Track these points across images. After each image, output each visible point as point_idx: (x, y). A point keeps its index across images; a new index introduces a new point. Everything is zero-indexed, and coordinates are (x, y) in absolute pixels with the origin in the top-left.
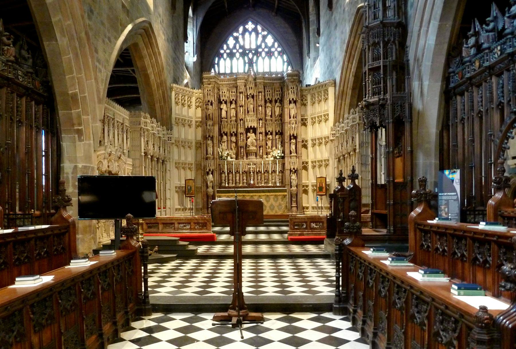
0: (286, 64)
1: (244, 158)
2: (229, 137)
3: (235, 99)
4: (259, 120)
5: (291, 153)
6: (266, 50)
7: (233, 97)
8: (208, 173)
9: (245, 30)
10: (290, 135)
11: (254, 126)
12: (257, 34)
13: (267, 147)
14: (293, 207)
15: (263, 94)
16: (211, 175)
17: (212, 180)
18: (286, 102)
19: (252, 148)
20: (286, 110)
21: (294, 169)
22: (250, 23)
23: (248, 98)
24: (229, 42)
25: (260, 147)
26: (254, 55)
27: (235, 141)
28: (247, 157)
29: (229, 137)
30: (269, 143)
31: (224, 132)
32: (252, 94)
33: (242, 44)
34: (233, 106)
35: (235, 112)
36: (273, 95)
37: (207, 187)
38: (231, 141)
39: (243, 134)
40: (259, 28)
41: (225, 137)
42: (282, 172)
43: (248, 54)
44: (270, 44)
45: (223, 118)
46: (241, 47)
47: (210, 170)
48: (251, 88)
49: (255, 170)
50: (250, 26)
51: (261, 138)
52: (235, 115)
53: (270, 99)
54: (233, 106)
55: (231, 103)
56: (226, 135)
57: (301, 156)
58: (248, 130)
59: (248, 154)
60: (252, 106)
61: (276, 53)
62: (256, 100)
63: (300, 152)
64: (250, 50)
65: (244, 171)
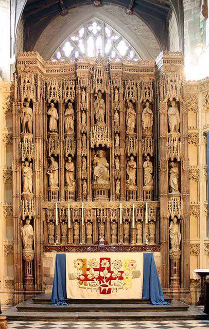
1: (88, 198)
2: (62, 163)
3: (72, 99)
4: (115, 134)
5: (170, 192)
7: (69, 95)
8: (24, 223)
9: (88, 33)
10: (170, 159)
11: (105, 145)
12: (105, 38)
13: (129, 181)
14: (173, 280)
15: (121, 91)
16: (30, 226)
17: (32, 234)
18: (162, 105)
20: (162, 117)
21: (176, 216)
22: (95, 24)
23: (96, 98)
24: (64, 49)
25: (116, 180)
27: (73, 170)
28: (93, 196)
29: (62, 163)
30: (132, 176)
31: (53, 155)
32: (103, 91)
33: (82, 50)
34: (70, 111)
35: (72, 122)
36: (139, 94)
37: (23, 247)
38: (65, 169)
39: (86, 158)
40: (108, 31)
41: (55, 164)
42: (157, 221)
45: (51, 132)
47: (27, 217)
48: (101, 80)
49: (108, 219)
50: (95, 28)
51: (118, 165)
52: (72, 127)
53: (134, 101)
54: (70, 111)
55: (66, 107)
56: (57, 159)
57: (189, 196)
58: (95, 150)
60: (102, 112)
62: (111, 102)
63: (186, 189)
65: (88, 221)
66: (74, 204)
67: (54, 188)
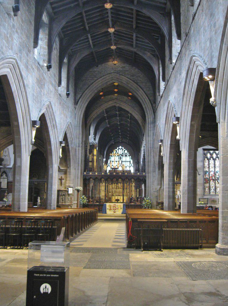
0: (131, 159)
6: (125, 154)
9: (119, 149)
12: (122, 150)
19: (120, 187)
22: (120, 146)
26: (121, 156)
33: (118, 152)
40: (123, 148)
43: (119, 156)
44: (126, 153)
46: (118, 153)
50: (120, 147)
59: (119, 188)
61: (128, 156)
64: (120, 154)
66: (116, 190)
67: (113, 187)
